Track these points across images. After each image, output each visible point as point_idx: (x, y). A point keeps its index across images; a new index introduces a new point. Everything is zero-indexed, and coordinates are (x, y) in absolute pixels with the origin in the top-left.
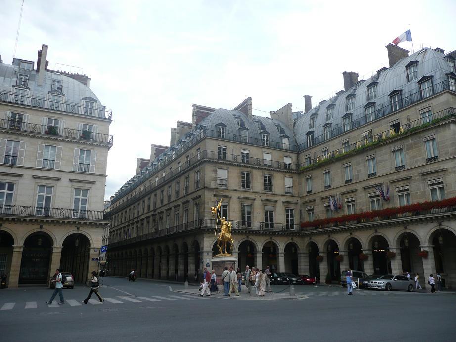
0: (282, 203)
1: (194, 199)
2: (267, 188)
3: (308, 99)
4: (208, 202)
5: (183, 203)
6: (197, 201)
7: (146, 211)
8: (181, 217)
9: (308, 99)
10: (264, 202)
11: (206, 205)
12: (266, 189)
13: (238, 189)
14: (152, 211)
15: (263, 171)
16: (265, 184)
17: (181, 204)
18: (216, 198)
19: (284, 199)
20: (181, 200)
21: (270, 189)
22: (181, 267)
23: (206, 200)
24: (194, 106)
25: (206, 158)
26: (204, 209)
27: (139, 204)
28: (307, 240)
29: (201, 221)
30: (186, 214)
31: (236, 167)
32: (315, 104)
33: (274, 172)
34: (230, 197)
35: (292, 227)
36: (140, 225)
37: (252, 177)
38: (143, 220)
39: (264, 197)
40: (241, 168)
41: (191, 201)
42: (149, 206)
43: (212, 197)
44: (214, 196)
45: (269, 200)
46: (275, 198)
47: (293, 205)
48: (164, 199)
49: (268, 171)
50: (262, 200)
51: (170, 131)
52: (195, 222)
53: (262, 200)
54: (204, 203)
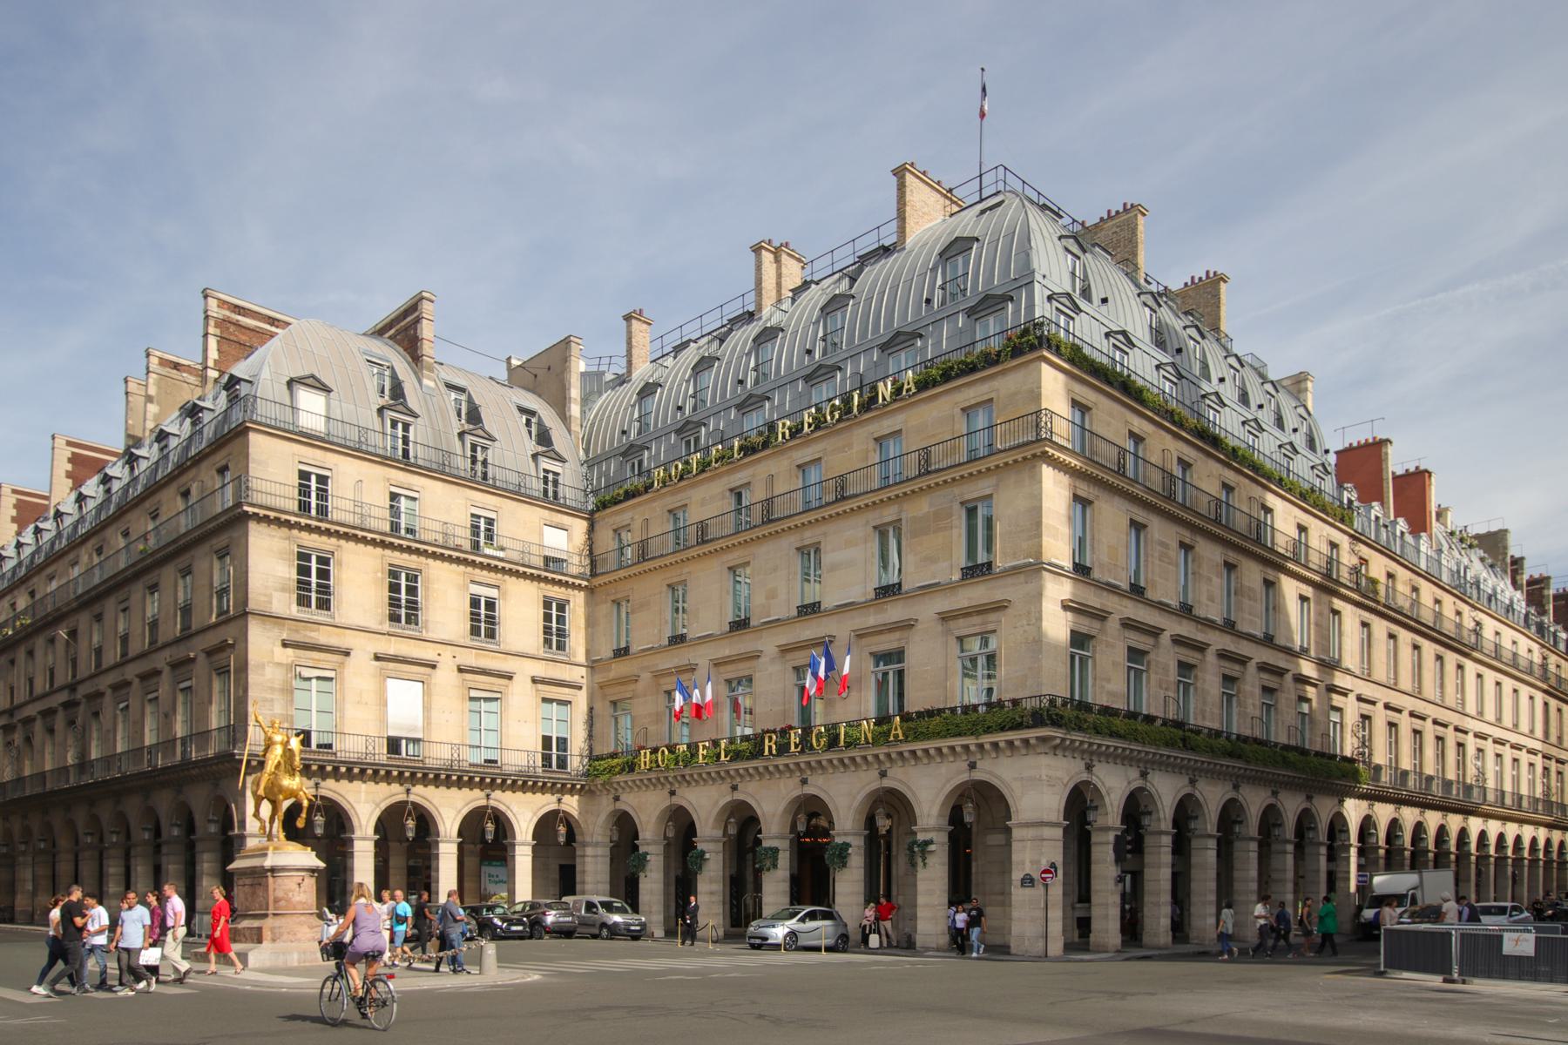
4: (262, 666)
5: (175, 666)
7: (38, 690)
13: (374, 626)
14: (61, 689)
16: (475, 617)
17: (167, 670)
18: (290, 651)
20: (166, 653)
27: (12, 662)
28: (605, 806)
29: (236, 729)
31: (370, 548)
34: (347, 654)
35: (562, 763)
37: (427, 589)
38: (28, 721)
40: (388, 552)
41: (202, 658)
43: (279, 649)
54: (243, 667)
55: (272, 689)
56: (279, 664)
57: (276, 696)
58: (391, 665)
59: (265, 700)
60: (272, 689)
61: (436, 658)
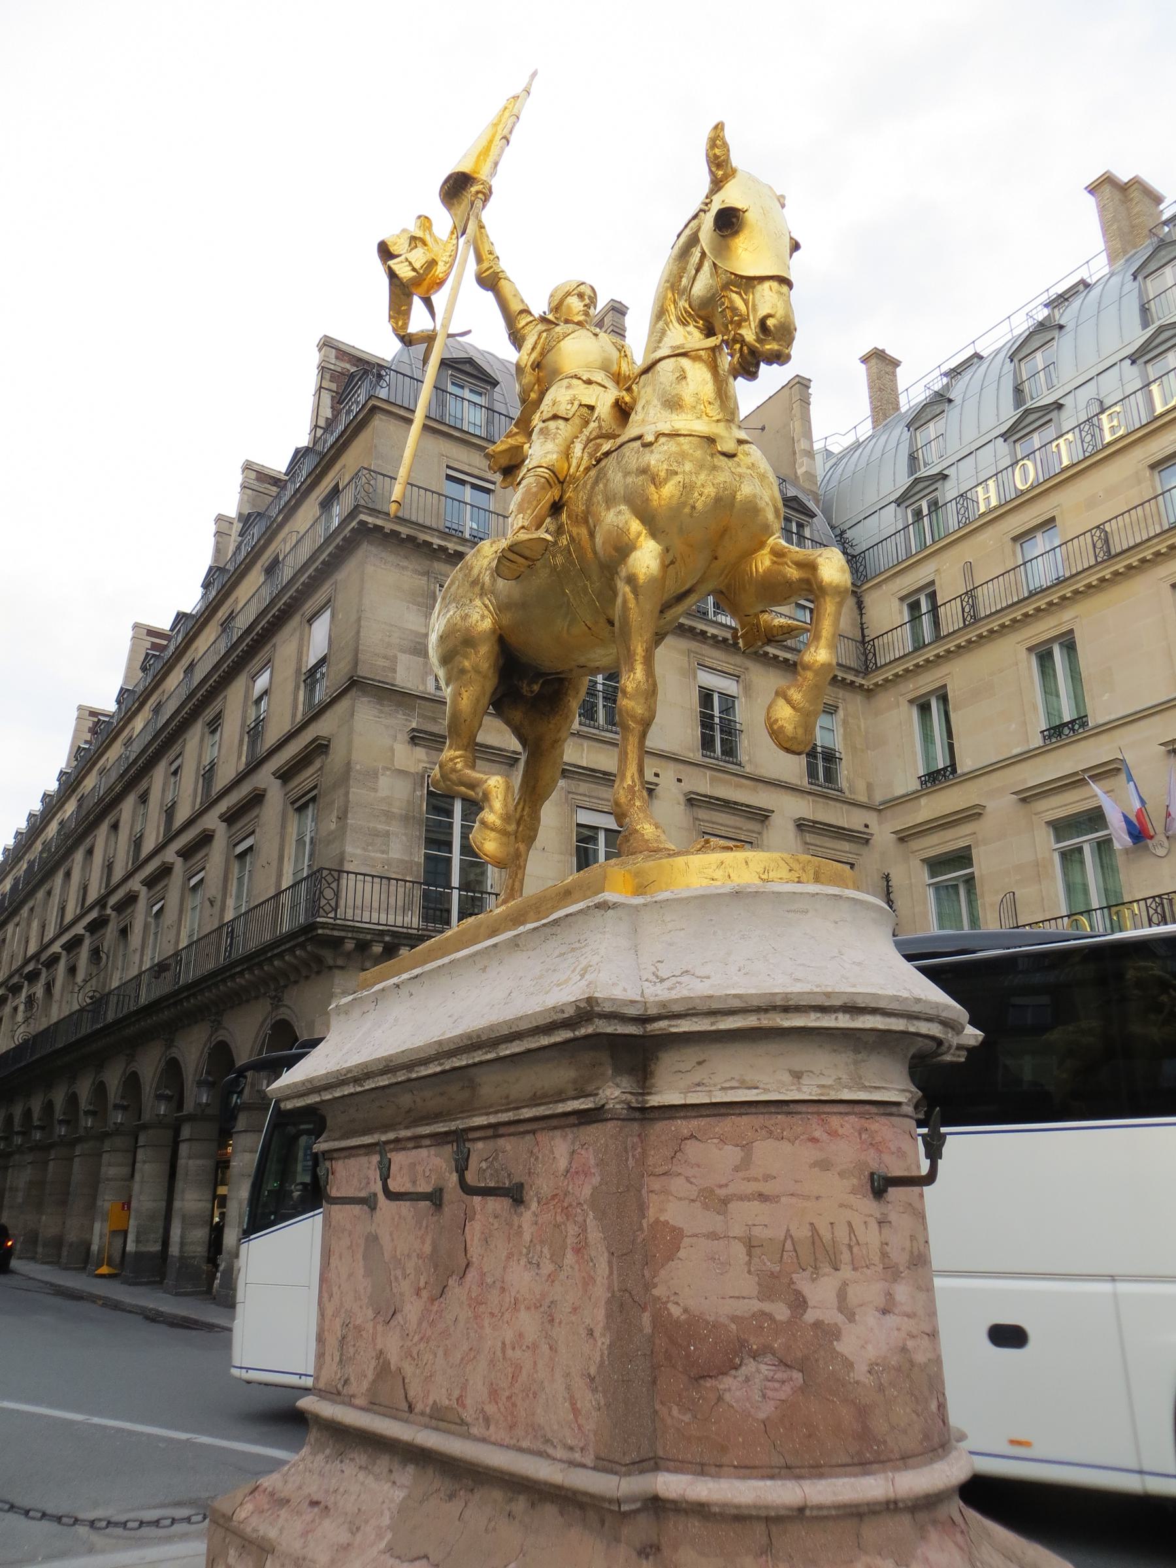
0: (791, 827)
1: (285, 776)
2: (713, 738)
3: (881, 363)
4: (373, 775)
6: (305, 778)
8: (212, 903)
9: (881, 363)
10: (703, 814)
11: (357, 792)
12: (707, 743)
14: (91, 908)
15: (694, 645)
16: (706, 722)
18: (420, 753)
19: (803, 808)
21: (730, 750)
22: (191, 1200)
23: (361, 759)
24: (327, 343)
25: (374, 512)
26: (342, 818)
29: (323, 878)
30: (240, 879)
32: (912, 390)
33: (749, 664)
36: (39, 990)
39: (703, 784)
42: (85, 889)
44: (416, 738)
45: (727, 806)
46: (761, 798)
47: (846, 846)
48: (146, 834)
49: (717, 654)
50: (693, 801)
51: (212, 528)
52: (285, 898)
53: (693, 801)
55: (388, 815)
56: (402, 773)
57: (395, 828)
58: (584, 787)
59: (376, 834)
60: (388, 815)
61: (655, 780)
